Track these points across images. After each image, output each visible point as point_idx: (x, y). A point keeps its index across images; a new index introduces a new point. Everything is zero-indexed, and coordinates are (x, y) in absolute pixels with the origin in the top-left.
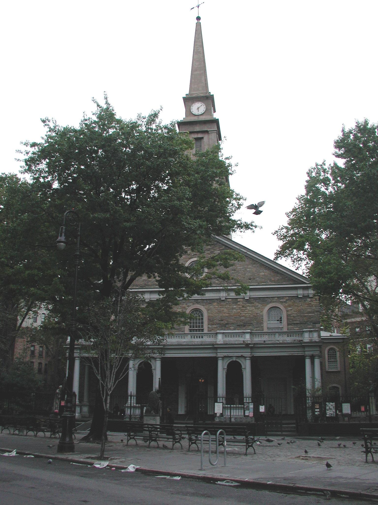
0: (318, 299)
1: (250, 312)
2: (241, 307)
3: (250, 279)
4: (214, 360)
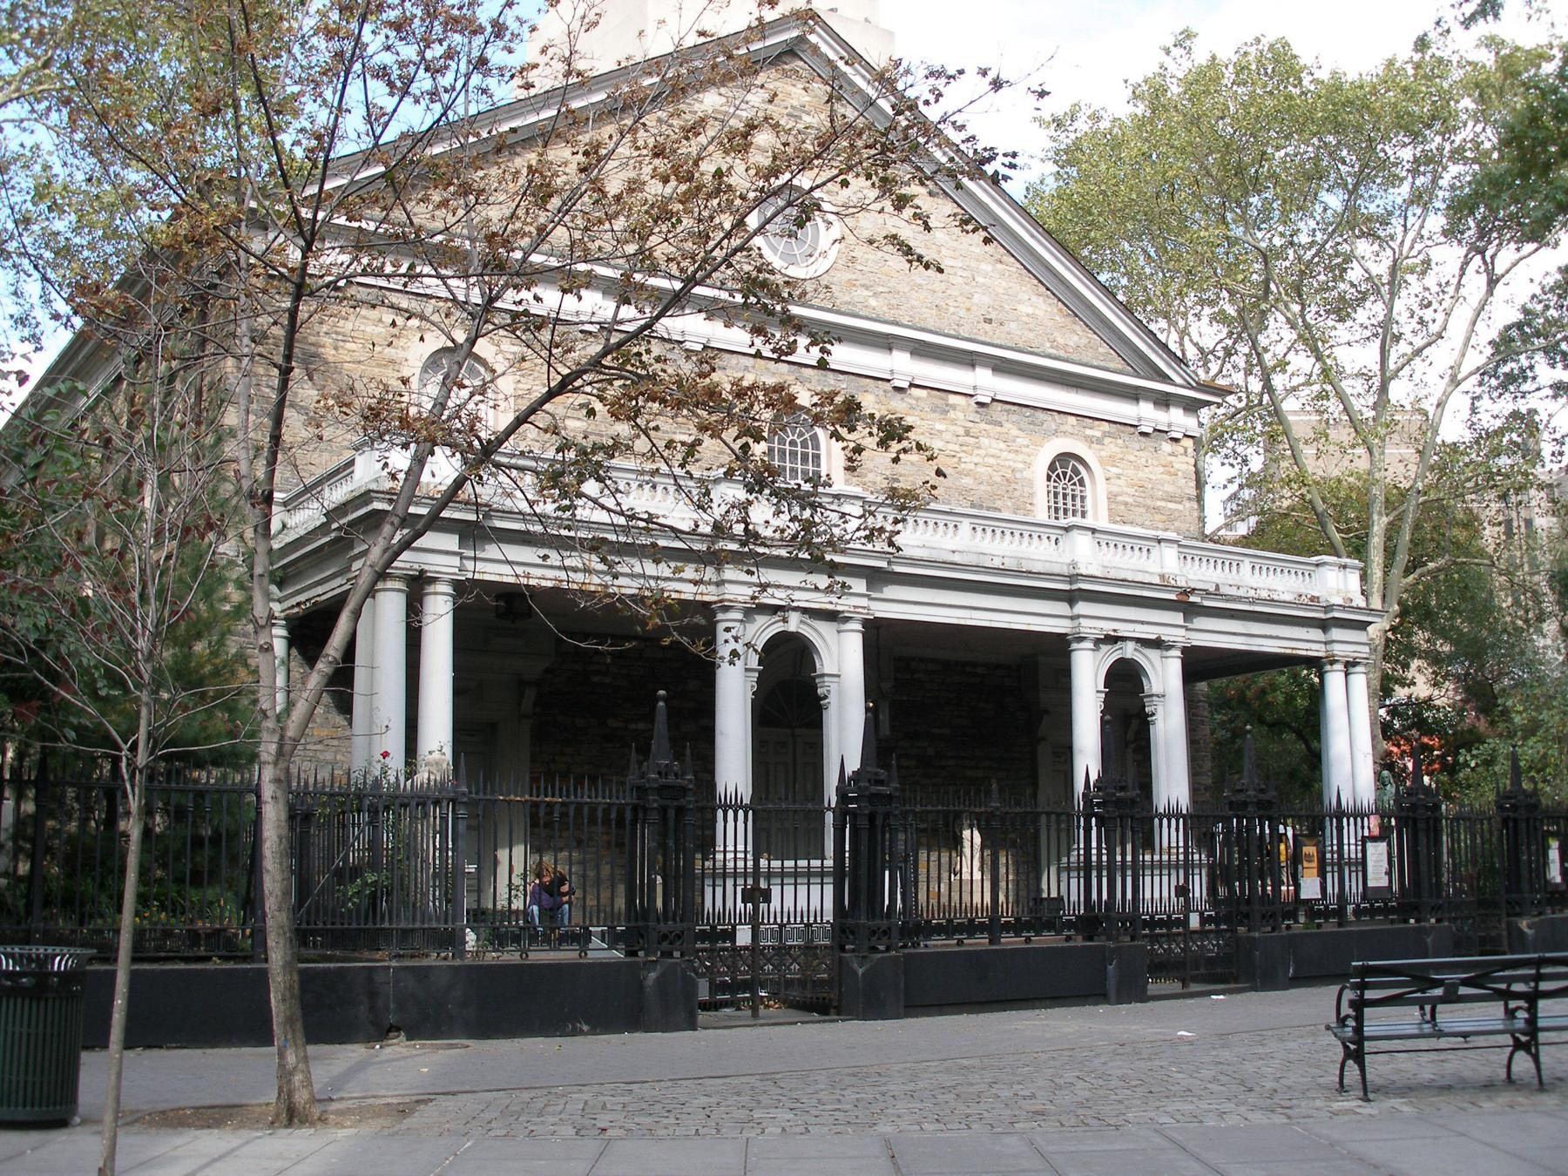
0: (1190, 451)
1: (992, 461)
2: (961, 431)
3: (990, 321)
4: (1057, 650)
